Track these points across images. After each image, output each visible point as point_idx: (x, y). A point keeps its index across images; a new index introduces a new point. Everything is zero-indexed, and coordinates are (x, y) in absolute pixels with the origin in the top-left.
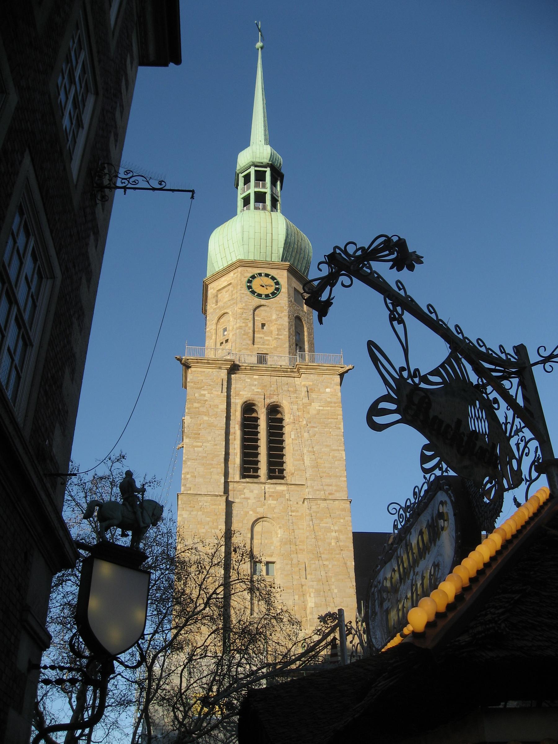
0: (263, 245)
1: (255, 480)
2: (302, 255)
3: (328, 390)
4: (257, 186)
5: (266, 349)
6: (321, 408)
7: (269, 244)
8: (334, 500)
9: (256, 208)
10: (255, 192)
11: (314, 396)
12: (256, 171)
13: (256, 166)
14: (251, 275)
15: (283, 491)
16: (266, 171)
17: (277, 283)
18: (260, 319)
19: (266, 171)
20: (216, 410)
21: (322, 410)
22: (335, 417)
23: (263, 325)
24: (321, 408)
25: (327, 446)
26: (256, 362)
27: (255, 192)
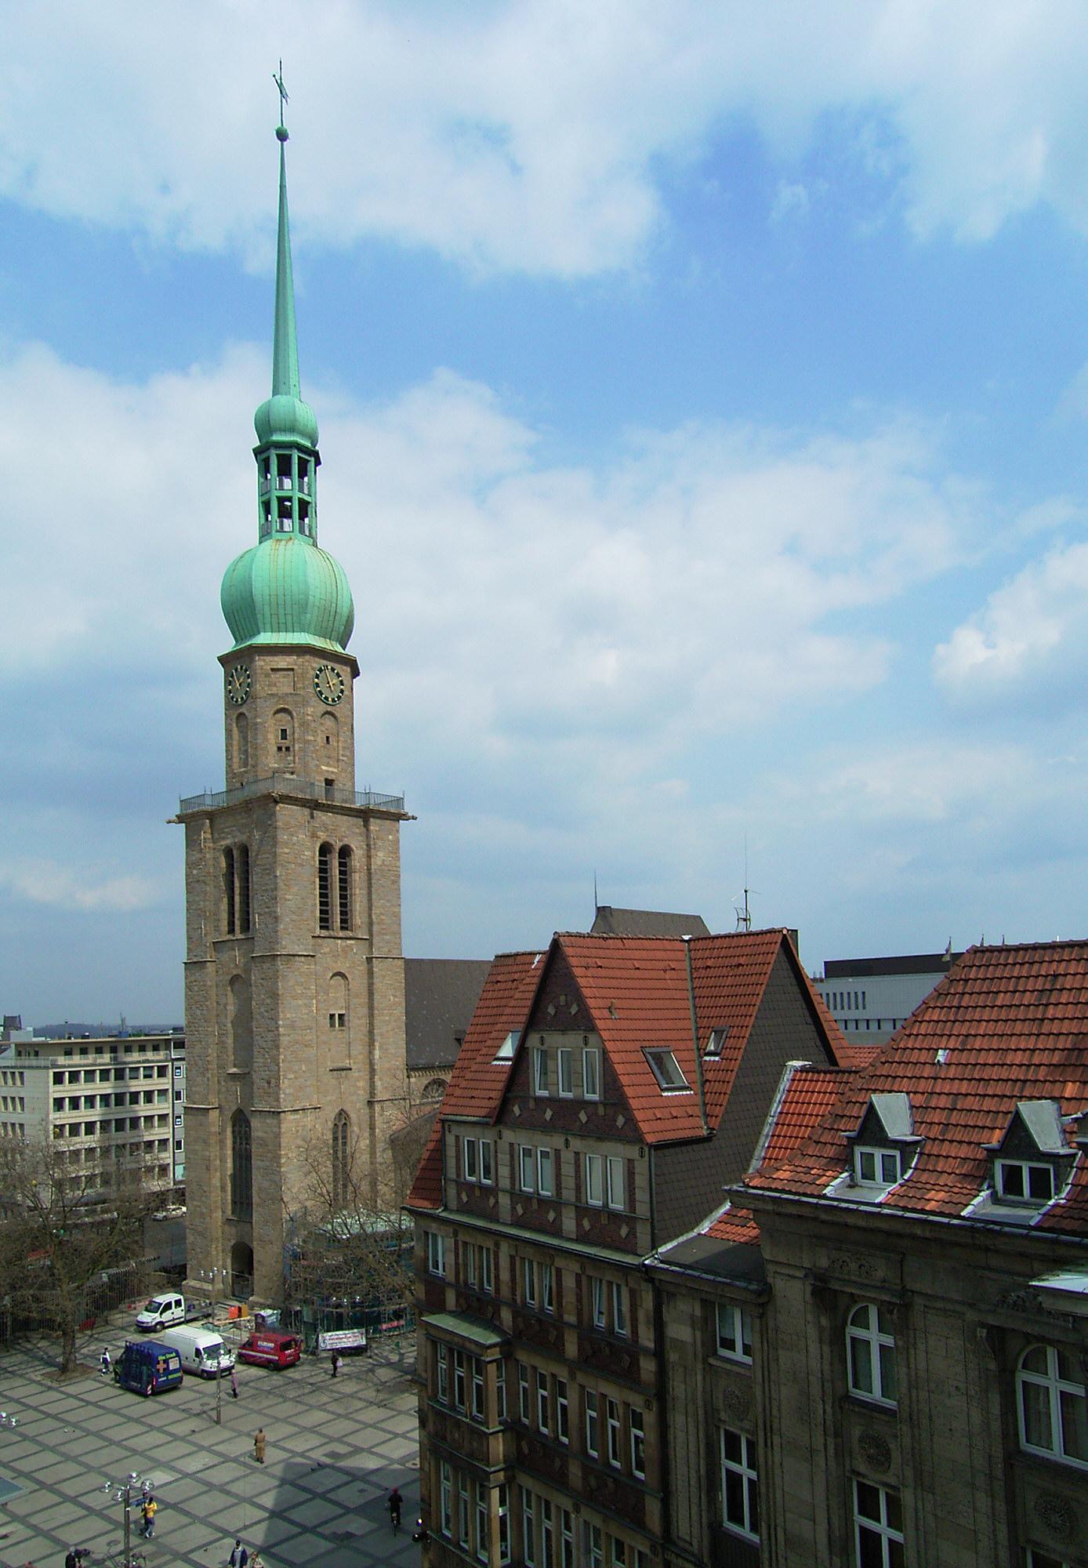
16: (309, 461)
25: (388, 901)
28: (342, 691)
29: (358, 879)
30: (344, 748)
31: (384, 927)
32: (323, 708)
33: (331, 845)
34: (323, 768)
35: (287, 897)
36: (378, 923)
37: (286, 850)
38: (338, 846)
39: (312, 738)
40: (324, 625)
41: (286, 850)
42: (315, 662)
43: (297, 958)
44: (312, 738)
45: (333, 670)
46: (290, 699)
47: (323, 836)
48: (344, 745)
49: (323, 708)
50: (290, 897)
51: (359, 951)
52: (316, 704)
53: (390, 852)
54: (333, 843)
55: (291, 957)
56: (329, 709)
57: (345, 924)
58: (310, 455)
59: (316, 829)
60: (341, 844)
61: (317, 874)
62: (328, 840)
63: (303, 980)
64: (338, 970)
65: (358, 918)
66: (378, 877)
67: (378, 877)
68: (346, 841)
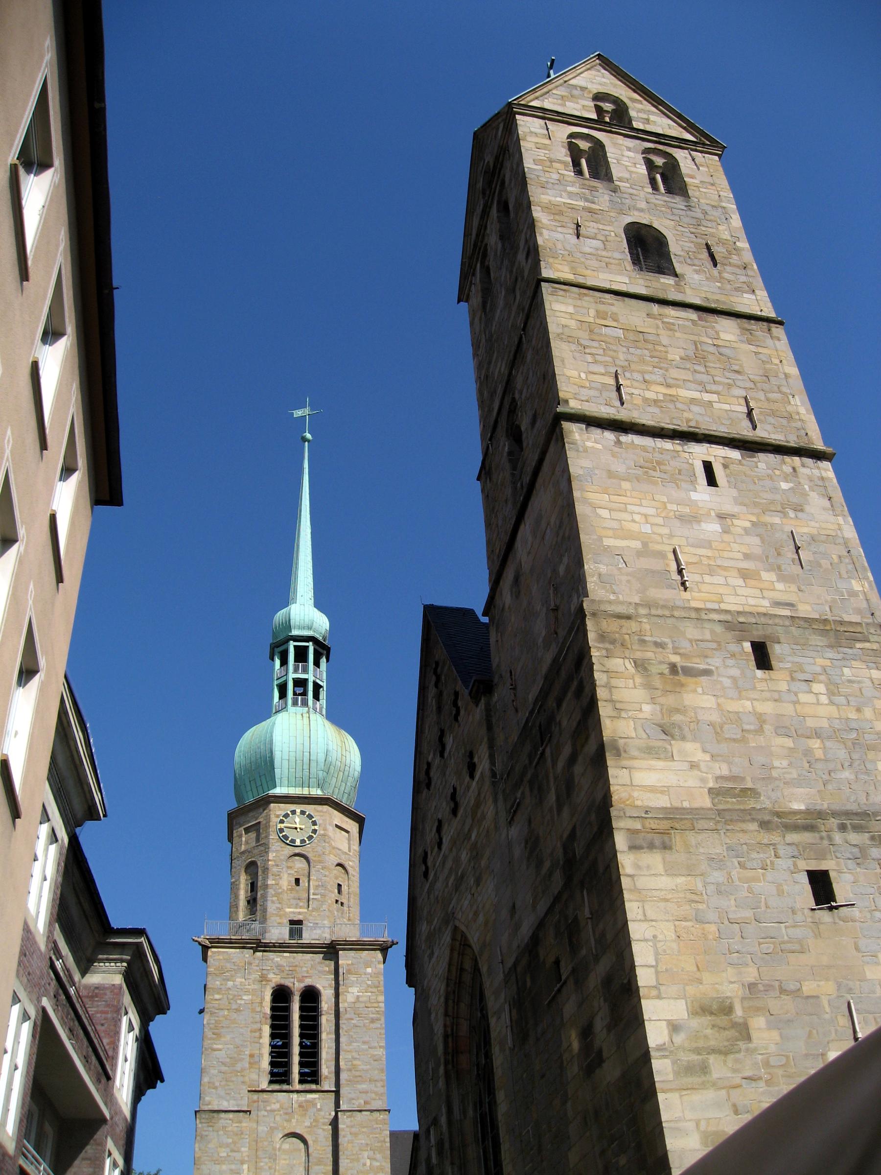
0: (299, 767)
1: (285, 1087)
2: (346, 773)
3: (369, 970)
4: (296, 670)
5: (300, 913)
6: (361, 994)
7: (306, 767)
8: (372, 1111)
9: (295, 703)
10: (293, 679)
11: (353, 979)
12: (295, 647)
13: (295, 640)
14: (283, 813)
15: (315, 1099)
16: (308, 647)
17: (314, 823)
18: (293, 872)
19: (308, 647)
20: (239, 1002)
21: (362, 996)
22: (376, 1005)
23: (297, 881)
24: (361, 994)
25: (364, 1043)
26: (287, 936)
27: (293, 679)
28: (315, 831)
29: (326, 1022)
30: (317, 887)
31: (358, 1074)
32: (290, 850)
33: (287, 987)
34: (288, 910)
35: (215, 1046)
36: (350, 1070)
37: (217, 997)
38: (297, 987)
39: (274, 882)
40: (299, 774)
41: (217, 997)
42: (280, 809)
43: (223, 1115)
44: (274, 882)
45: (303, 813)
46: (256, 851)
47: (275, 979)
48: (317, 883)
49: (290, 850)
50: (220, 1047)
51: (323, 1104)
52: (279, 848)
53: (369, 986)
54: (290, 985)
55: (215, 1115)
56: (297, 850)
57: (311, 1075)
58: (308, 642)
59: (265, 972)
60: (302, 985)
61: (269, 1021)
62: (283, 982)
63: (230, 1140)
64: (293, 1131)
65: (326, 1069)
66: (348, 1016)
67: (348, 1016)
68: (308, 982)
